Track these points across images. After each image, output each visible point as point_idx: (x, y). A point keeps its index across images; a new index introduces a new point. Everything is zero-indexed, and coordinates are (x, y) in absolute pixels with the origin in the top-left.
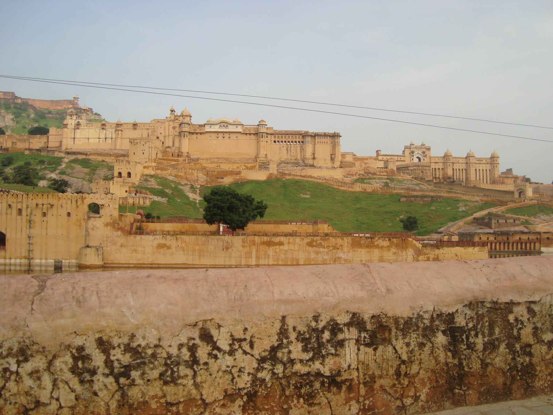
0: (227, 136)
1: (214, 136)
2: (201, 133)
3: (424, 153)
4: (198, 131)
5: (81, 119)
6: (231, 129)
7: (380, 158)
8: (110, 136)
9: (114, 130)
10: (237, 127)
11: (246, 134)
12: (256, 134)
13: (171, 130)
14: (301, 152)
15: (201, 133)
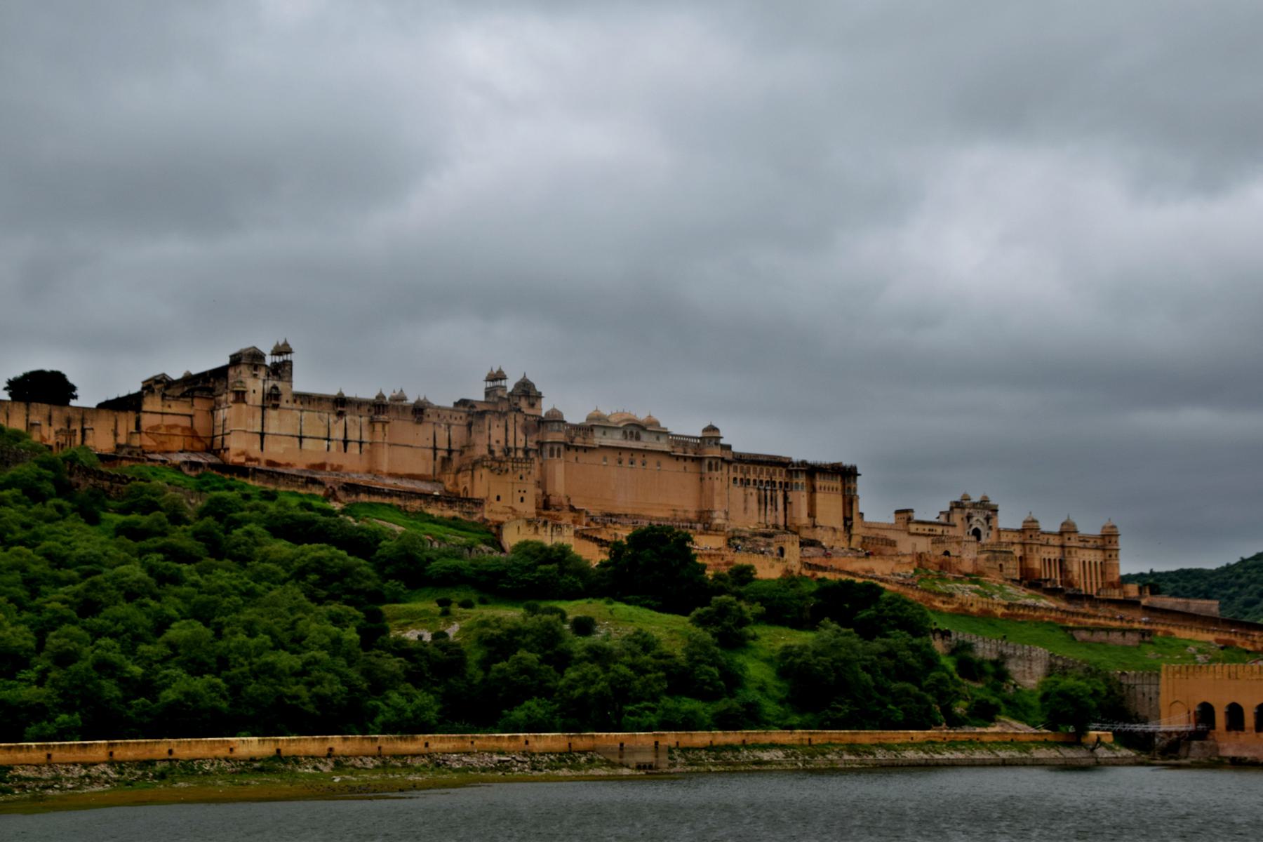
0: (638, 459)
1: (612, 458)
2: (586, 449)
3: (988, 519)
4: (579, 440)
5: (280, 379)
6: (647, 442)
7: (913, 528)
8: (357, 438)
9: (365, 420)
10: (658, 438)
11: (678, 458)
12: (698, 460)
13: (521, 436)
14: (785, 509)
15: (586, 449)
